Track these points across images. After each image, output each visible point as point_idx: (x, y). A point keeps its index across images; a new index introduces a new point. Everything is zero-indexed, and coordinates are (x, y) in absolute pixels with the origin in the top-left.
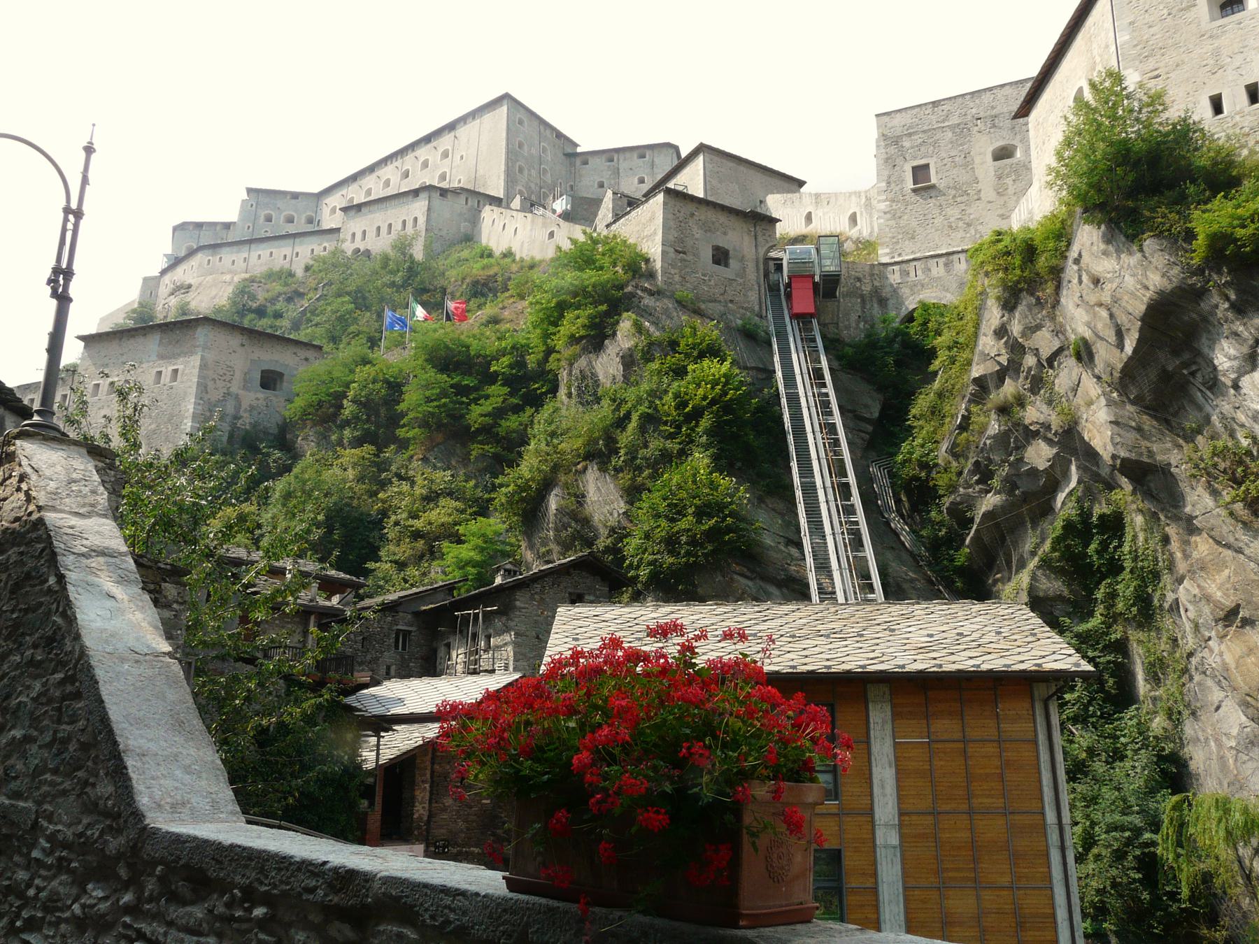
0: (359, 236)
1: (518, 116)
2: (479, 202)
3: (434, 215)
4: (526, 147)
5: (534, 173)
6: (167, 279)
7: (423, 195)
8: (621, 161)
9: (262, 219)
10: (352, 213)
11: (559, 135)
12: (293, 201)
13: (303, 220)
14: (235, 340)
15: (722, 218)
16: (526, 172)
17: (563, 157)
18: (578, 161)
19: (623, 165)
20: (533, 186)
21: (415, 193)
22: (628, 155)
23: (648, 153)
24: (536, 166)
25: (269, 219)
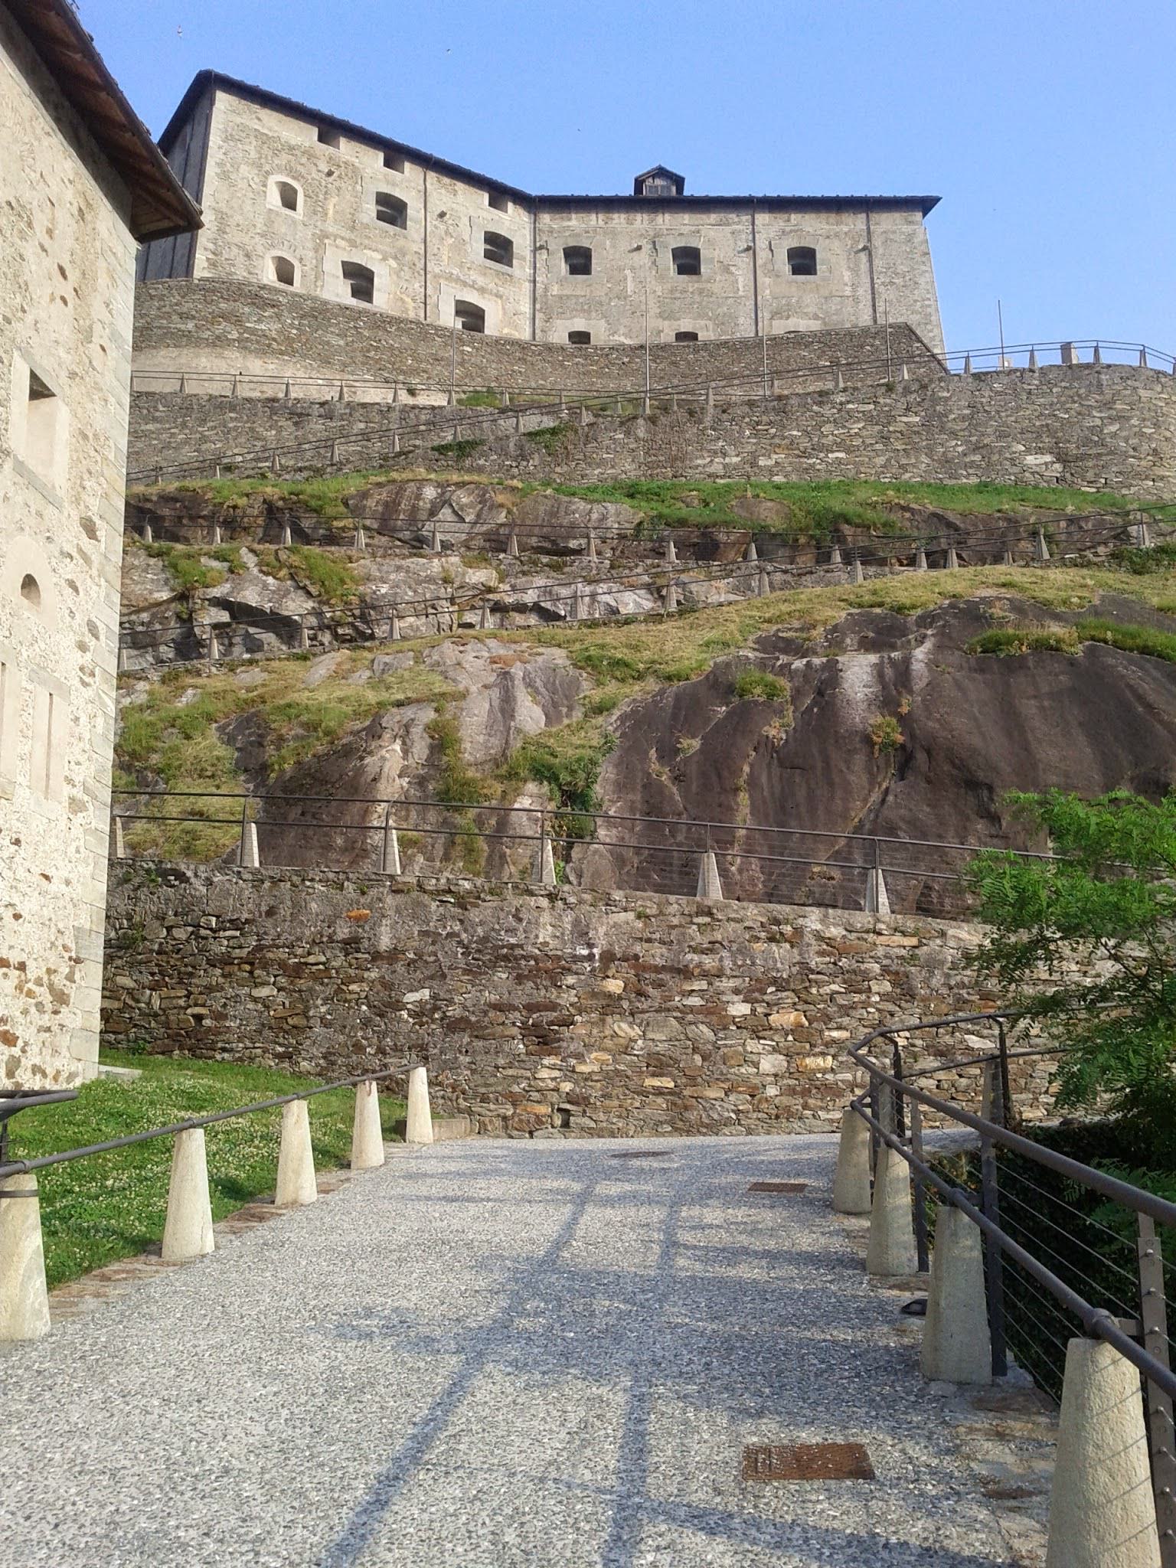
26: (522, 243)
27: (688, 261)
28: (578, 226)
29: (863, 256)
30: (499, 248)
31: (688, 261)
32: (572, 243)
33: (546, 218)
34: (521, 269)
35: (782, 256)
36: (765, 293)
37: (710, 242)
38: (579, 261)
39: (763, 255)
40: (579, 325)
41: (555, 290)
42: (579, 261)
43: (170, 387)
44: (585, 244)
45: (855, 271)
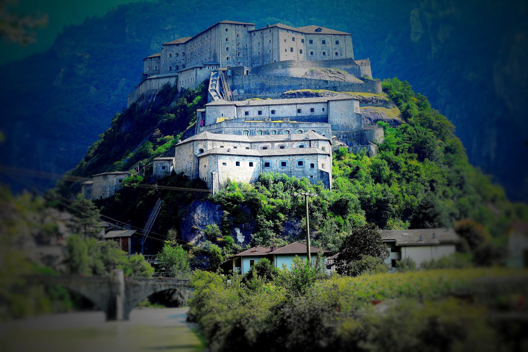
0: (182, 82)
1: (225, 28)
2: (213, 67)
3: (198, 77)
4: (229, 40)
5: (234, 47)
6: (141, 87)
7: (195, 70)
8: (264, 33)
9: (169, 56)
10: (180, 74)
11: (245, 26)
12: (178, 47)
13: (181, 54)
14: (113, 176)
15: (164, 161)
16: (230, 50)
17: (247, 34)
18: (253, 34)
19: (265, 36)
20: (233, 53)
21: (193, 68)
22: (266, 31)
23: (272, 30)
24: (235, 44)
25: (171, 55)
26: (305, 40)
27: (324, 42)
28: (310, 37)
29: (344, 42)
30: (303, 41)
31: (324, 42)
32: (310, 39)
33: (307, 35)
34: (305, 43)
35: (335, 42)
36: (333, 47)
37: (327, 39)
38: (311, 42)
39: (333, 41)
40: (312, 51)
41: (309, 46)
42: (311, 42)
43: (296, 76)
44: (312, 39)
45: (343, 44)
